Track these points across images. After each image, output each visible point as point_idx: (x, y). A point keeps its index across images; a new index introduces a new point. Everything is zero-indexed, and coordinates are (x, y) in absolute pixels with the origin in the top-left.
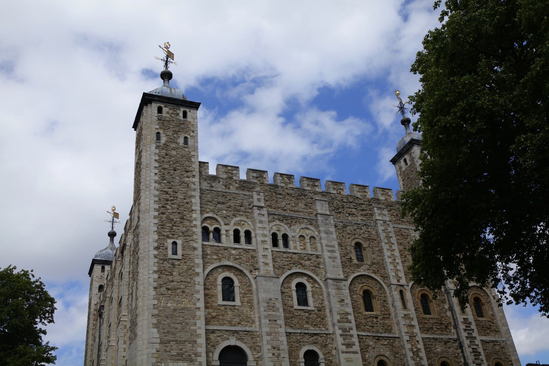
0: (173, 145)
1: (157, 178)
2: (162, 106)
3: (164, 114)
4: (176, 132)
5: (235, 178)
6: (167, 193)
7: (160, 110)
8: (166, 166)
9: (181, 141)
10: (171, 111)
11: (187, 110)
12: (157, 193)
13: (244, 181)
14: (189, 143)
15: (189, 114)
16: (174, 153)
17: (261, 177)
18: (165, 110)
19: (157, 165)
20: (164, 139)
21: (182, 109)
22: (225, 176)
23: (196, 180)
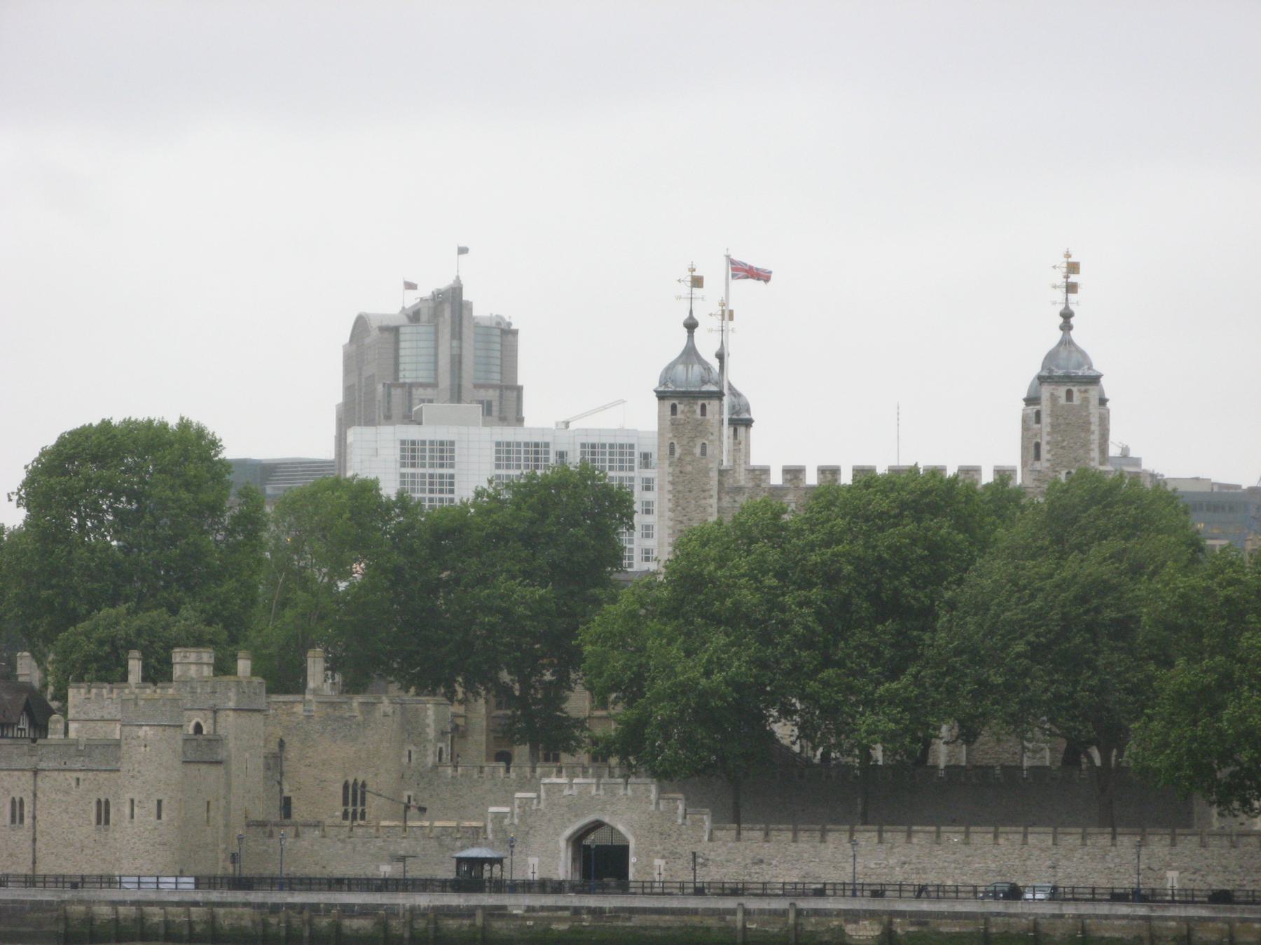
0: (688, 458)
1: (670, 505)
2: (676, 402)
3: (679, 416)
4: (692, 439)
5: (763, 485)
6: (681, 522)
7: (674, 408)
8: (680, 488)
9: (698, 451)
10: (687, 409)
11: (706, 402)
12: (671, 523)
13: (776, 488)
14: (709, 451)
15: (708, 407)
16: (689, 468)
17: (796, 478)
18: (680, 407)
19: (670, 488)
20: (678, 451)
21: (700, 402)
22: (751, 485)
23: (714, 501)
